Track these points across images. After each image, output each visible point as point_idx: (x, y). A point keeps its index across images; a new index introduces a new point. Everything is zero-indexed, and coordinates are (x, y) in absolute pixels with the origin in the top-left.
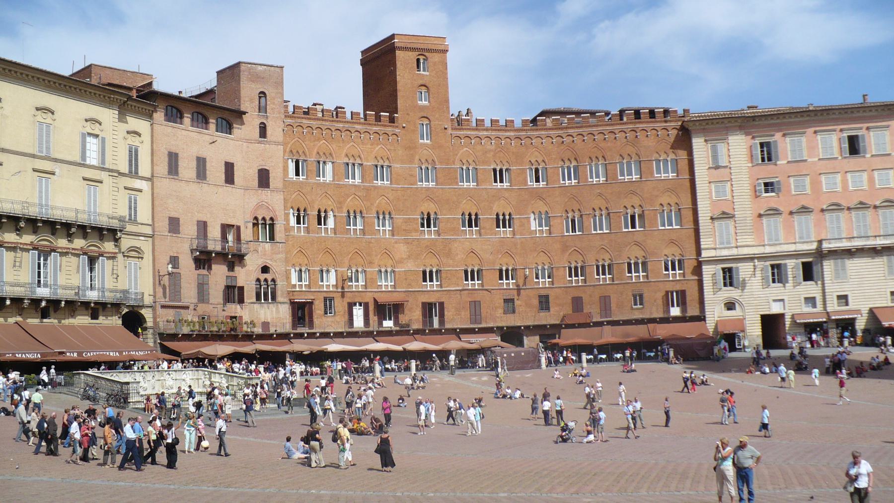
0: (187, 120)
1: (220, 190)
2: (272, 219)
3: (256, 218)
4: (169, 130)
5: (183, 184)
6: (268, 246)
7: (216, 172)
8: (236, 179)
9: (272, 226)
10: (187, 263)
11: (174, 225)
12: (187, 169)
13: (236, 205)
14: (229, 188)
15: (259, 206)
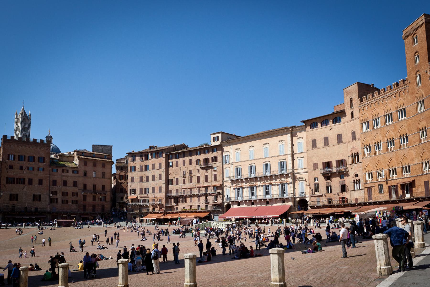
0: (319, 125)
1: (335, 147)
2: (358, 153)
3: (352, 154)
4: (312, 132)
5: (319, 150)
6: (356, 165)
7: (333, 140)
8: (343, 140)
9: (358, 156)
10: (321, 179)
11: (315, 166)
12: (320, 143)
13: (343, 152)
14: (340, 145)
15: (353, 148)
